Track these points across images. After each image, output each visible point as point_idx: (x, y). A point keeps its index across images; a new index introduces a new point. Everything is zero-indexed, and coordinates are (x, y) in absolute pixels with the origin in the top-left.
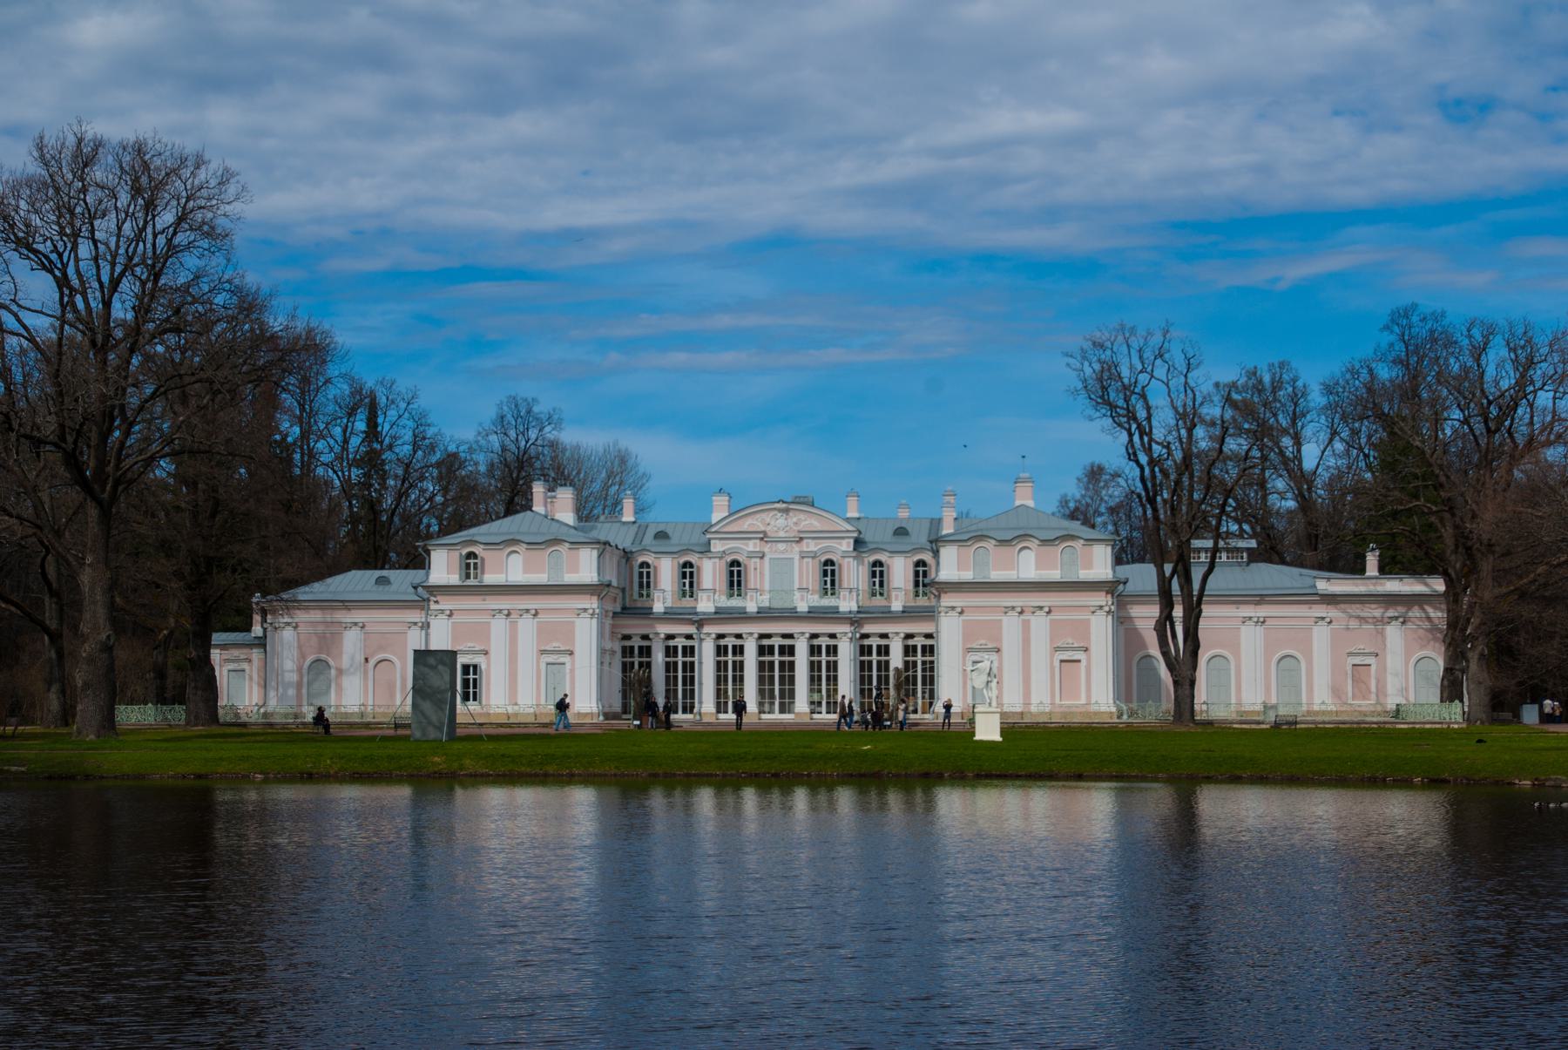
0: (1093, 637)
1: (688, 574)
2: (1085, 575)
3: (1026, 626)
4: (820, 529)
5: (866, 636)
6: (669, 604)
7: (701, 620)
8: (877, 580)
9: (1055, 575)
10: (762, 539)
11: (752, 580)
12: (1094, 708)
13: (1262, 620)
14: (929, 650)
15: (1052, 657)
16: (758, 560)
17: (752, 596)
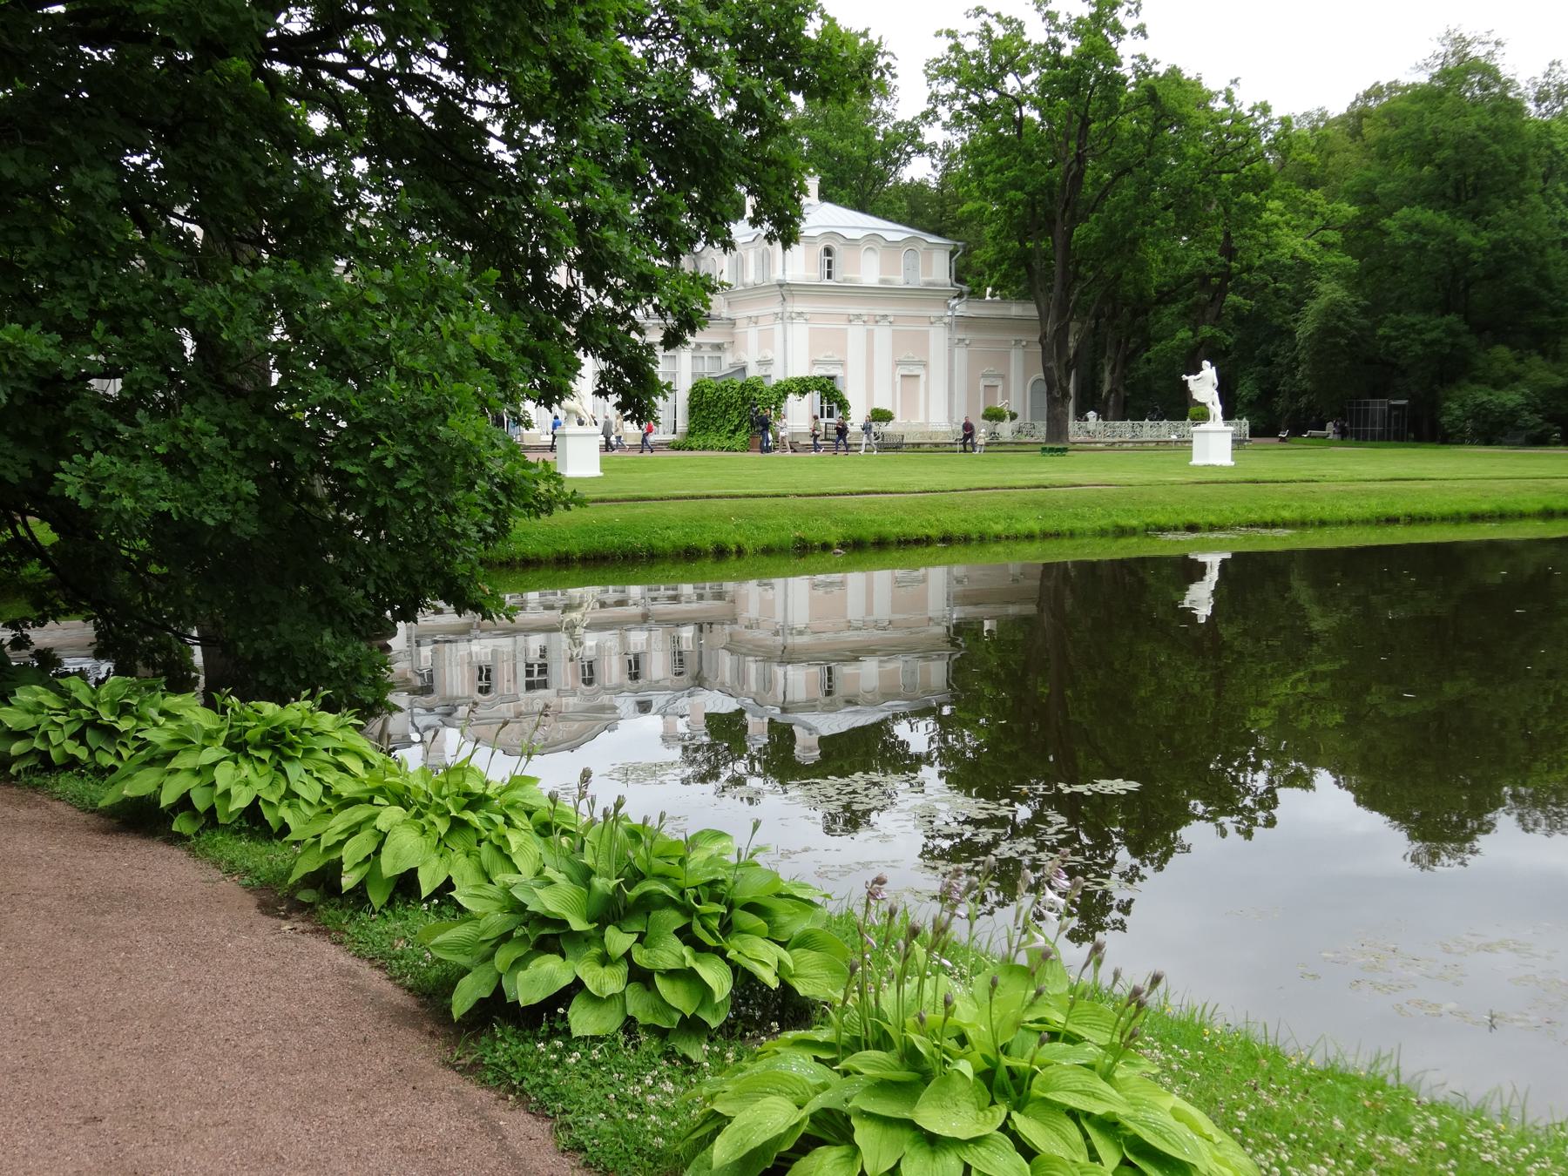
0: (932, 353)
3: (870, 334)
9: (899, 280)
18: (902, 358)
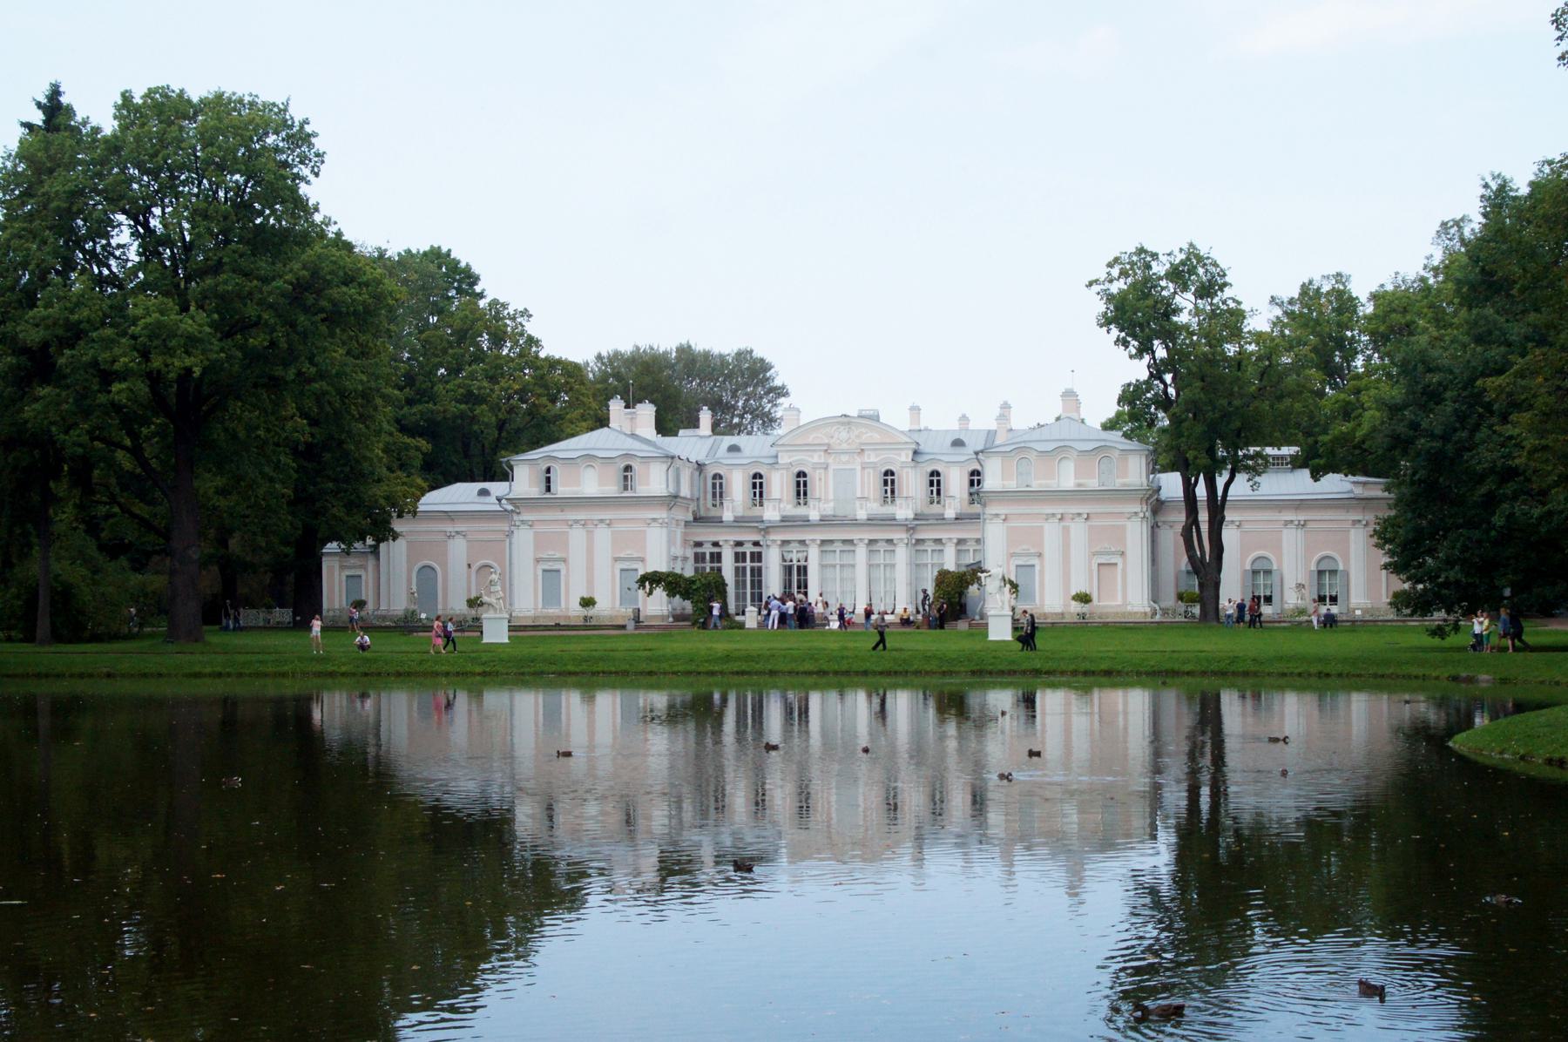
1: (757, 485)
2: (1118, 483)
3: (1066, 530)
5: (919, 541)
6: (740, 513)
7: (768, 527)
8: (935, 489)
9: (1093, 484)
10: (826, 450)
11: (816, 486)
12: (1129, 608)
13: (1302, 523)
16: (822, 471)
17: (814, 506)
18: (1098, 549)
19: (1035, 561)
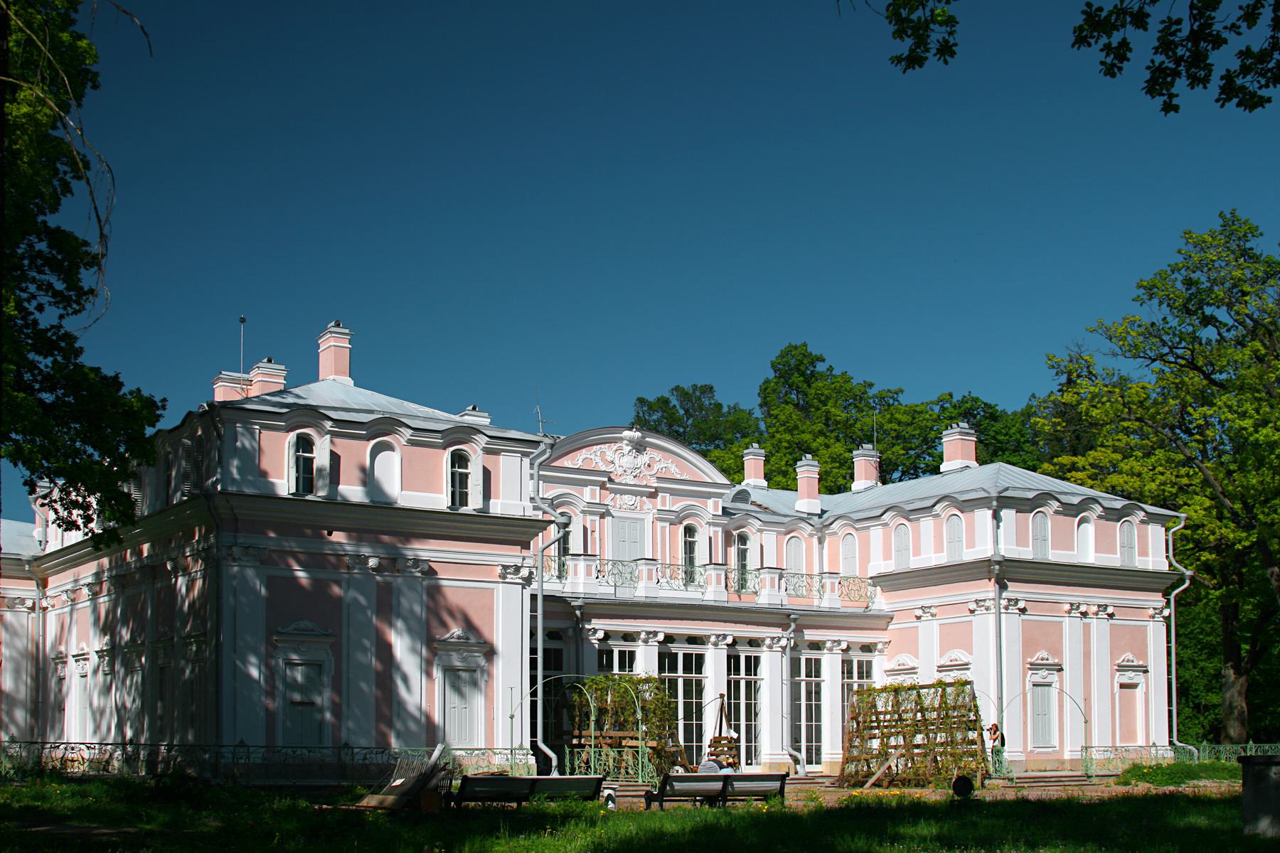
4: (678, 477)
14: (865, 670)
15: (1112, 677)
19: (1054, 677)
